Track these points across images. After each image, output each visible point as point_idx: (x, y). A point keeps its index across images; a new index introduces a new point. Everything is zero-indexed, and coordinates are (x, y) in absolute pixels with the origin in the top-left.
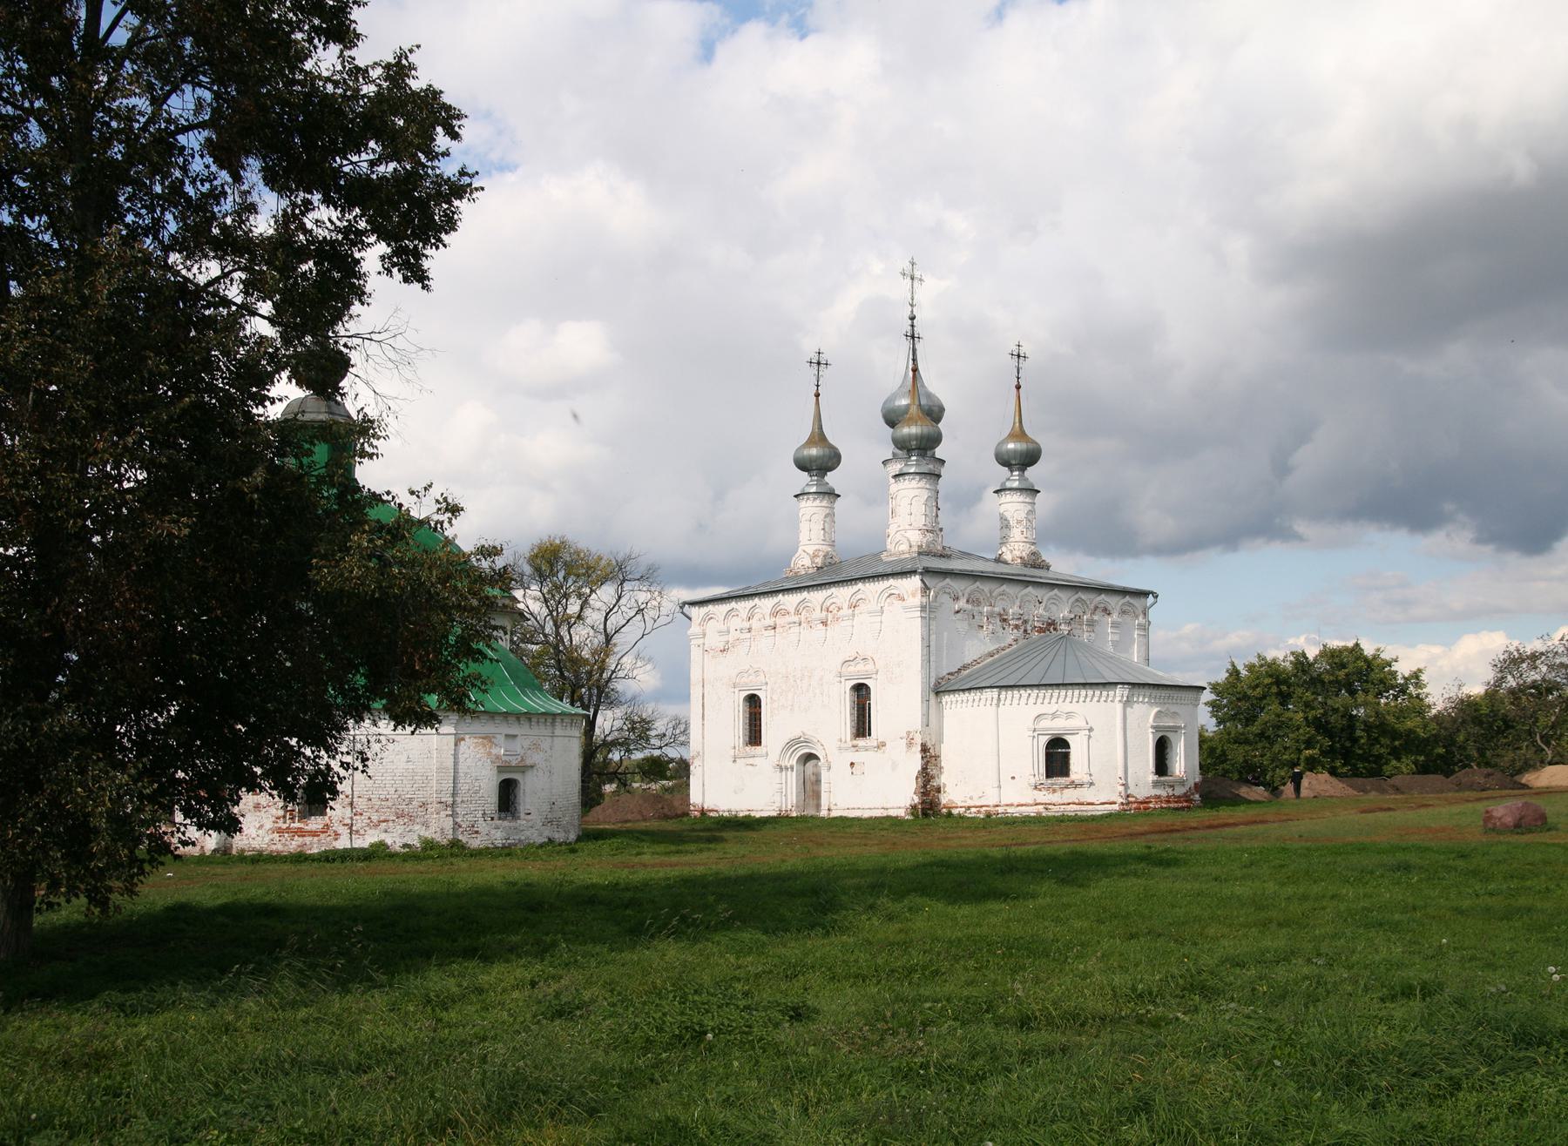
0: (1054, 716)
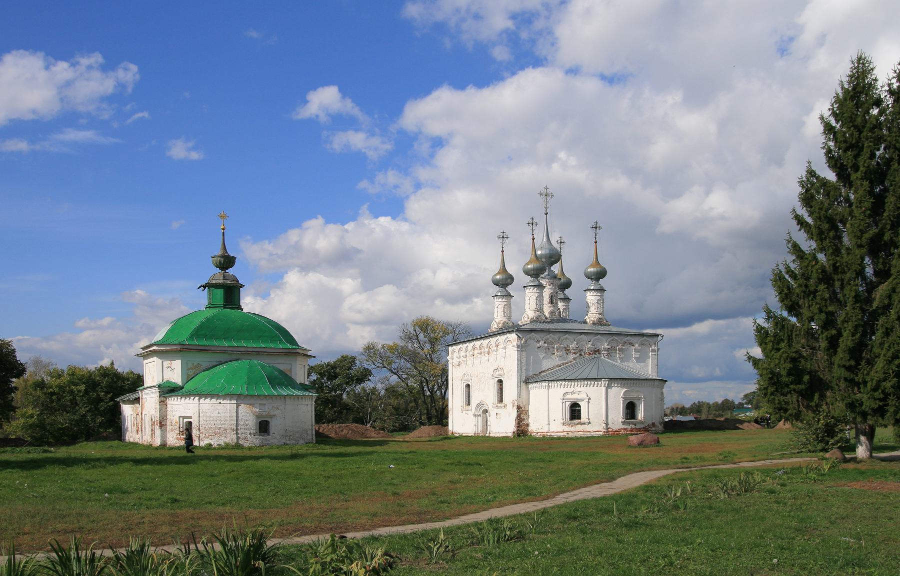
0: (572, 393)
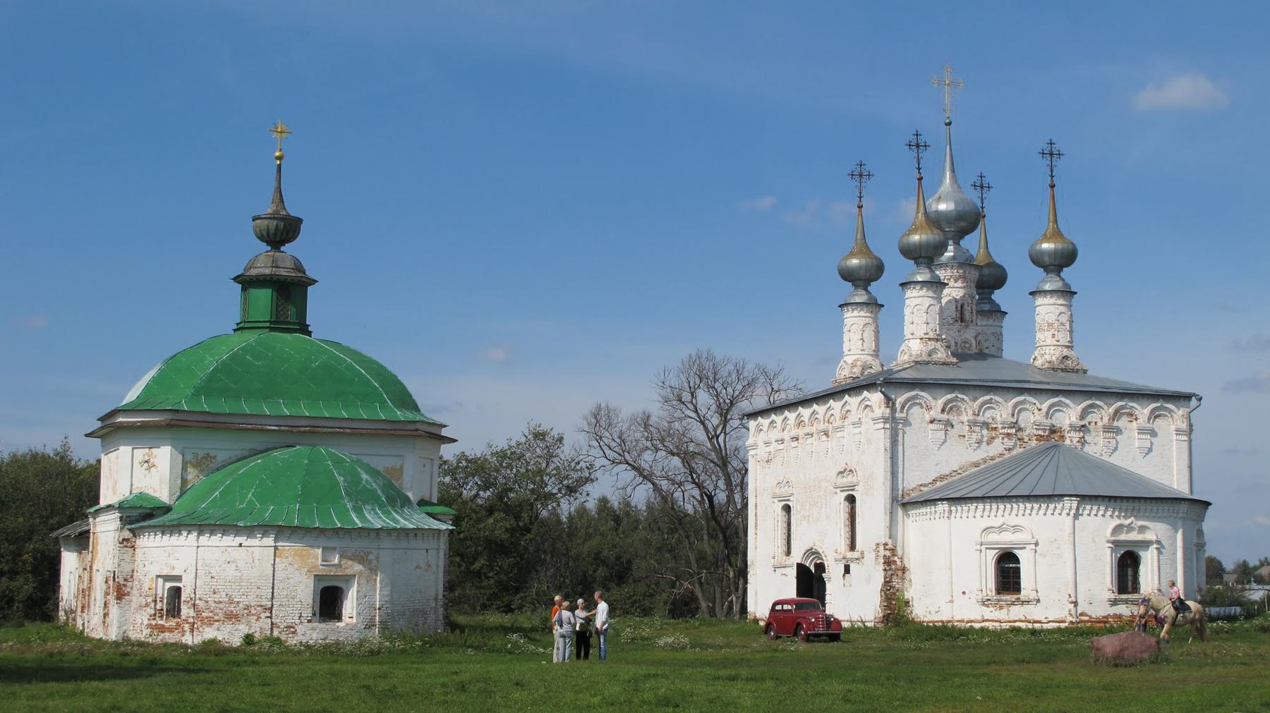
0: (1001, 529)
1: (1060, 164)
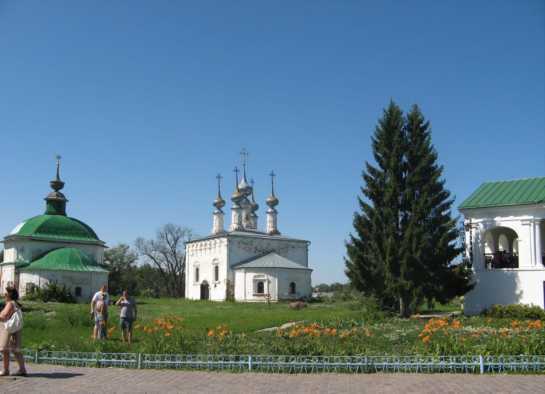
1: (274, 178)
